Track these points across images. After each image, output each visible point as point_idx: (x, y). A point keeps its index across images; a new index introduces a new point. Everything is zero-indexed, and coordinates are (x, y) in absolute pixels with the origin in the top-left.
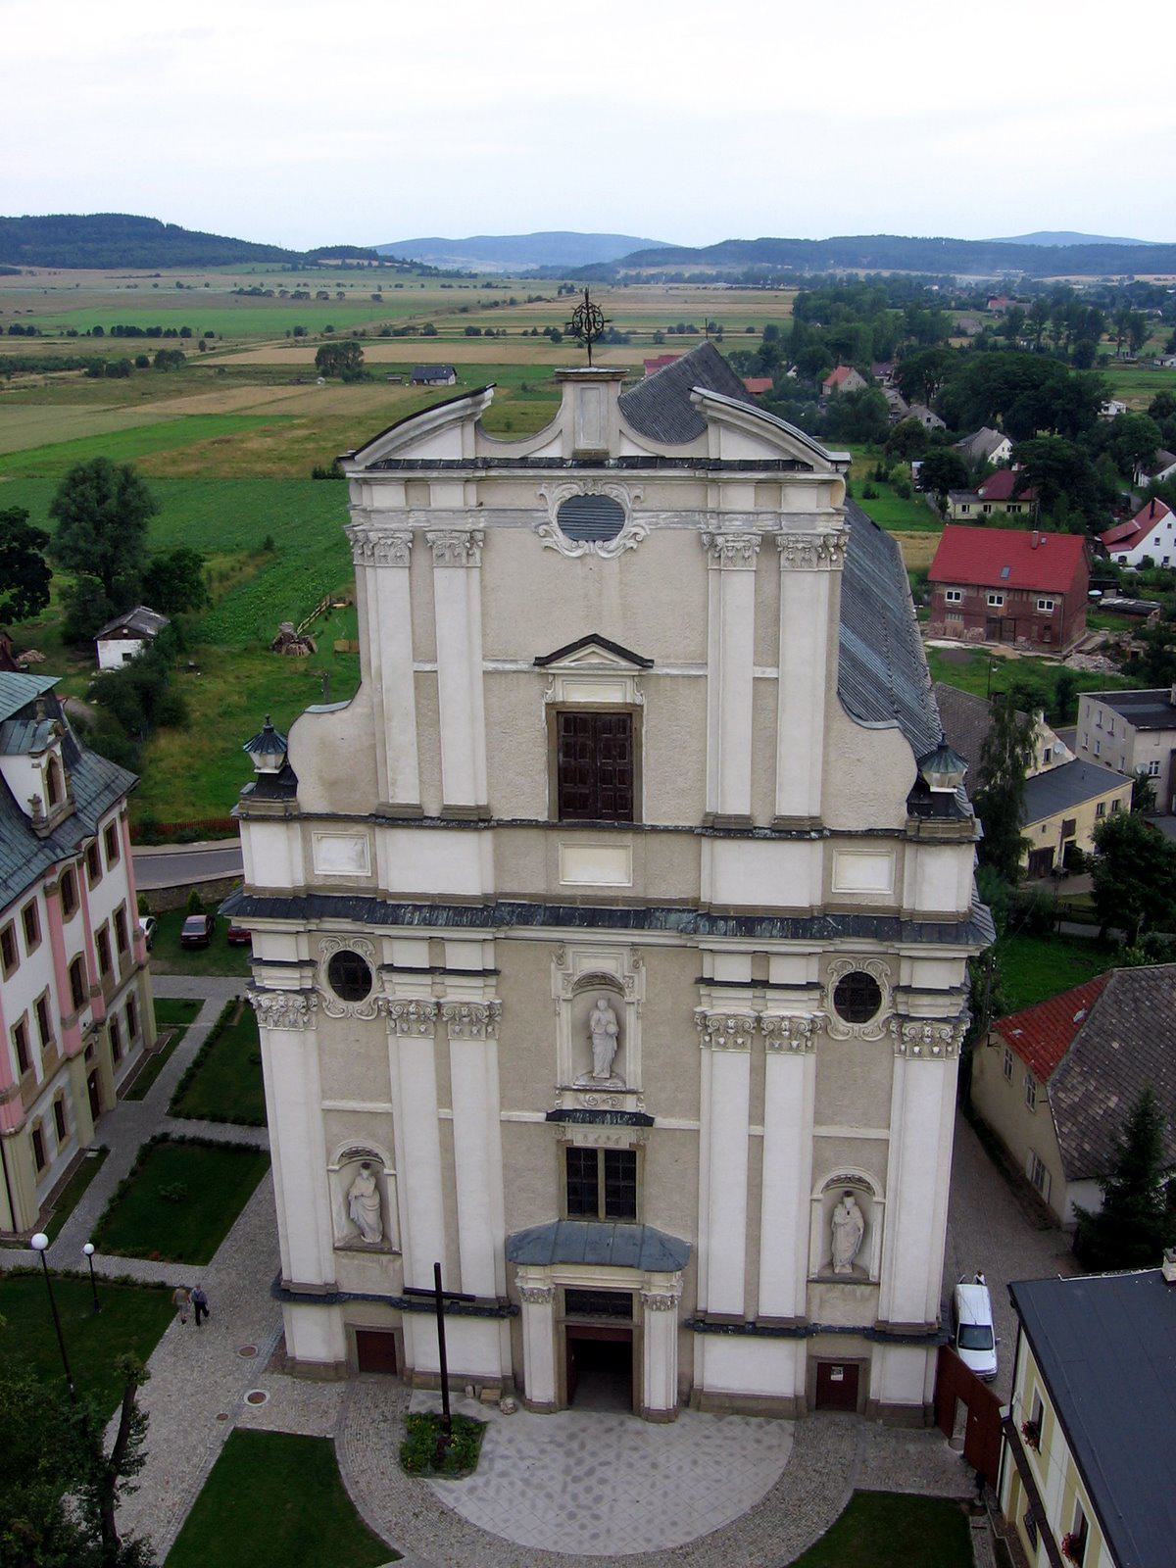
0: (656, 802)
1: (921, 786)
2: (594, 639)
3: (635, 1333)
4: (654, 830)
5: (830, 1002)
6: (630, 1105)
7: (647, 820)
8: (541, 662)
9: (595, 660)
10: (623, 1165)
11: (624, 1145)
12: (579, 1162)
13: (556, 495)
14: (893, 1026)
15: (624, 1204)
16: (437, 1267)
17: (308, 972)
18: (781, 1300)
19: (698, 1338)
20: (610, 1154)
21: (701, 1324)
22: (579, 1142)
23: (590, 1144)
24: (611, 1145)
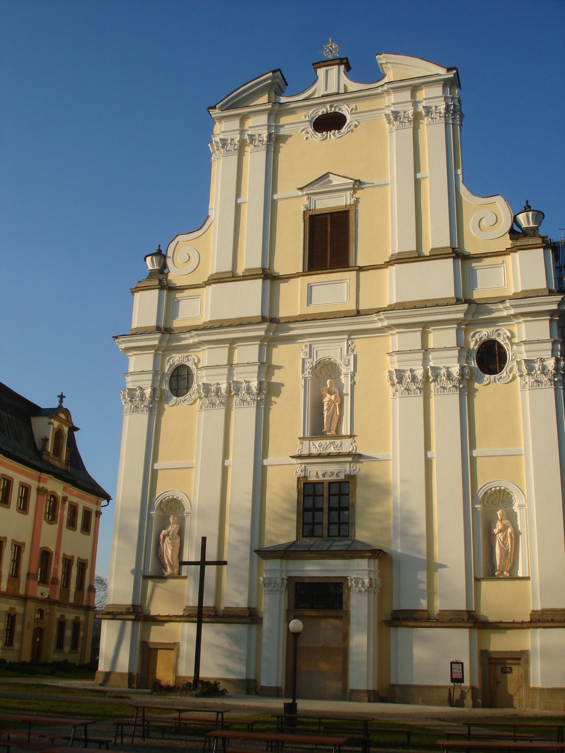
2: (329, 173)
4: (361, 269)
8: (301, 189)
11: (342, 477)
16: (204, 539)
19: (392, 630)
20: (330, 483)
23: (321, 478)
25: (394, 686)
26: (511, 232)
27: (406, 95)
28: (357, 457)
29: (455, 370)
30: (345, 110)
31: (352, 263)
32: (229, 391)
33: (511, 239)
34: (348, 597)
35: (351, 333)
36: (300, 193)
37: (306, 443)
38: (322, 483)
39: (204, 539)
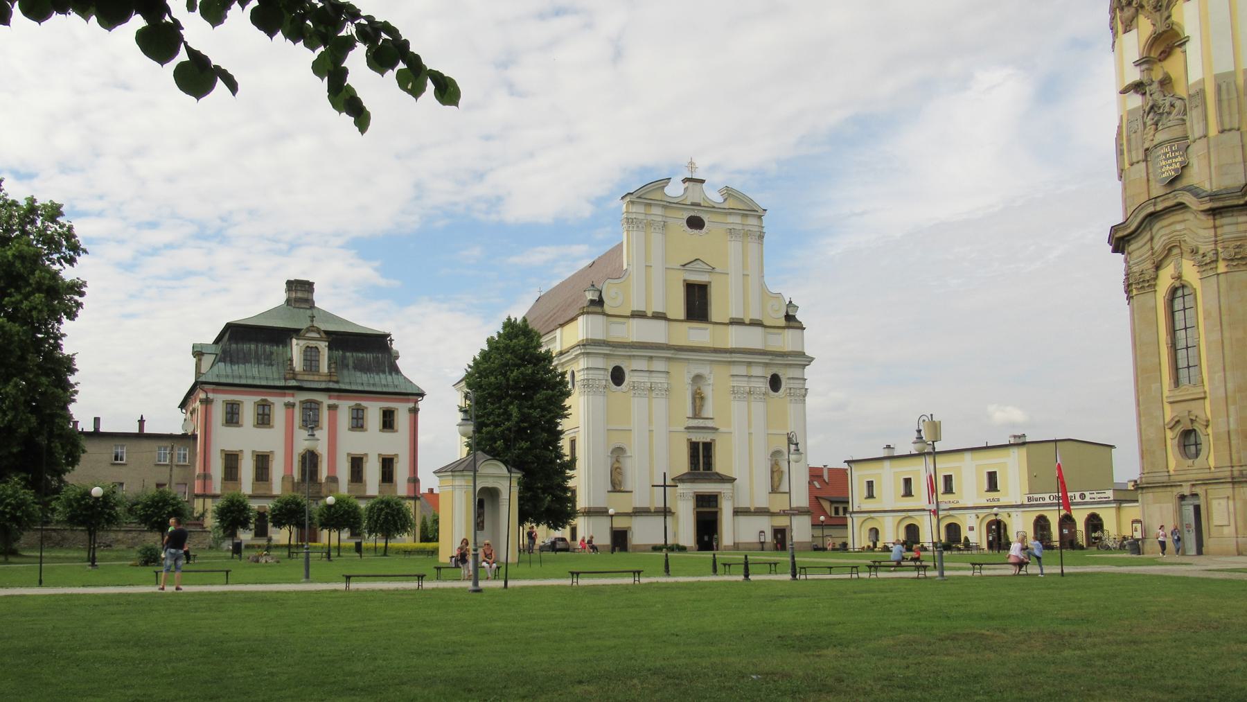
0: (716, 312)
1: (787, 312)
2: (697, 260)
3: (719, 513)
5: (768, 386)
6: (709, 424)
7: (713, 320)
9: (698, 266)
10: (708, 447)
11: (708, 440)
12: (694, 447)
13: (686, 215)
14: (788, 391)
15: (708, 464)
16: (665, 474)
17: (606, 373)
18: (761, 499)
19: (735, 517)
21: (737, 512)
22: (694, 440)
24: (705, 440)
25: (738, 543)
26: (785, 316)
27: (738, 220)
28: (715, 429)
29: (763, 390)
30: (705, 217)
31: (709, 320)
32: (651, 387)
33: (786, 320)
34: (721, 503)
35: (712, 361)
36: (682, 268)
37: (690, 420)
38: (698, 443)
39: (665, 474)
